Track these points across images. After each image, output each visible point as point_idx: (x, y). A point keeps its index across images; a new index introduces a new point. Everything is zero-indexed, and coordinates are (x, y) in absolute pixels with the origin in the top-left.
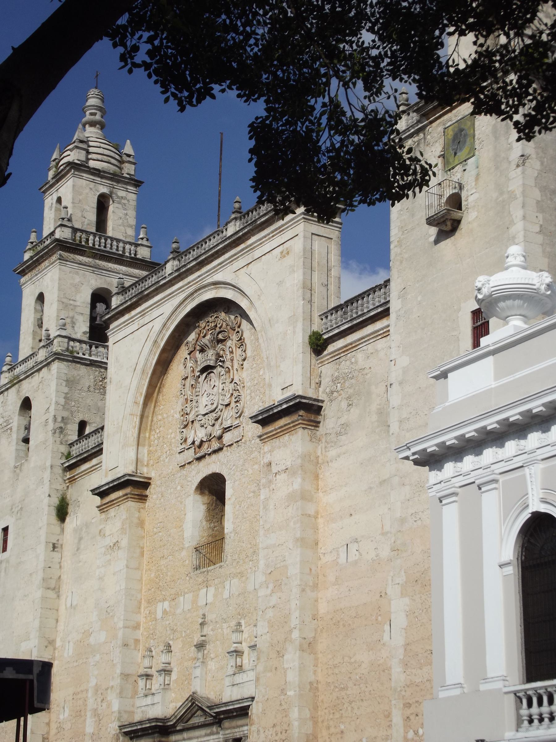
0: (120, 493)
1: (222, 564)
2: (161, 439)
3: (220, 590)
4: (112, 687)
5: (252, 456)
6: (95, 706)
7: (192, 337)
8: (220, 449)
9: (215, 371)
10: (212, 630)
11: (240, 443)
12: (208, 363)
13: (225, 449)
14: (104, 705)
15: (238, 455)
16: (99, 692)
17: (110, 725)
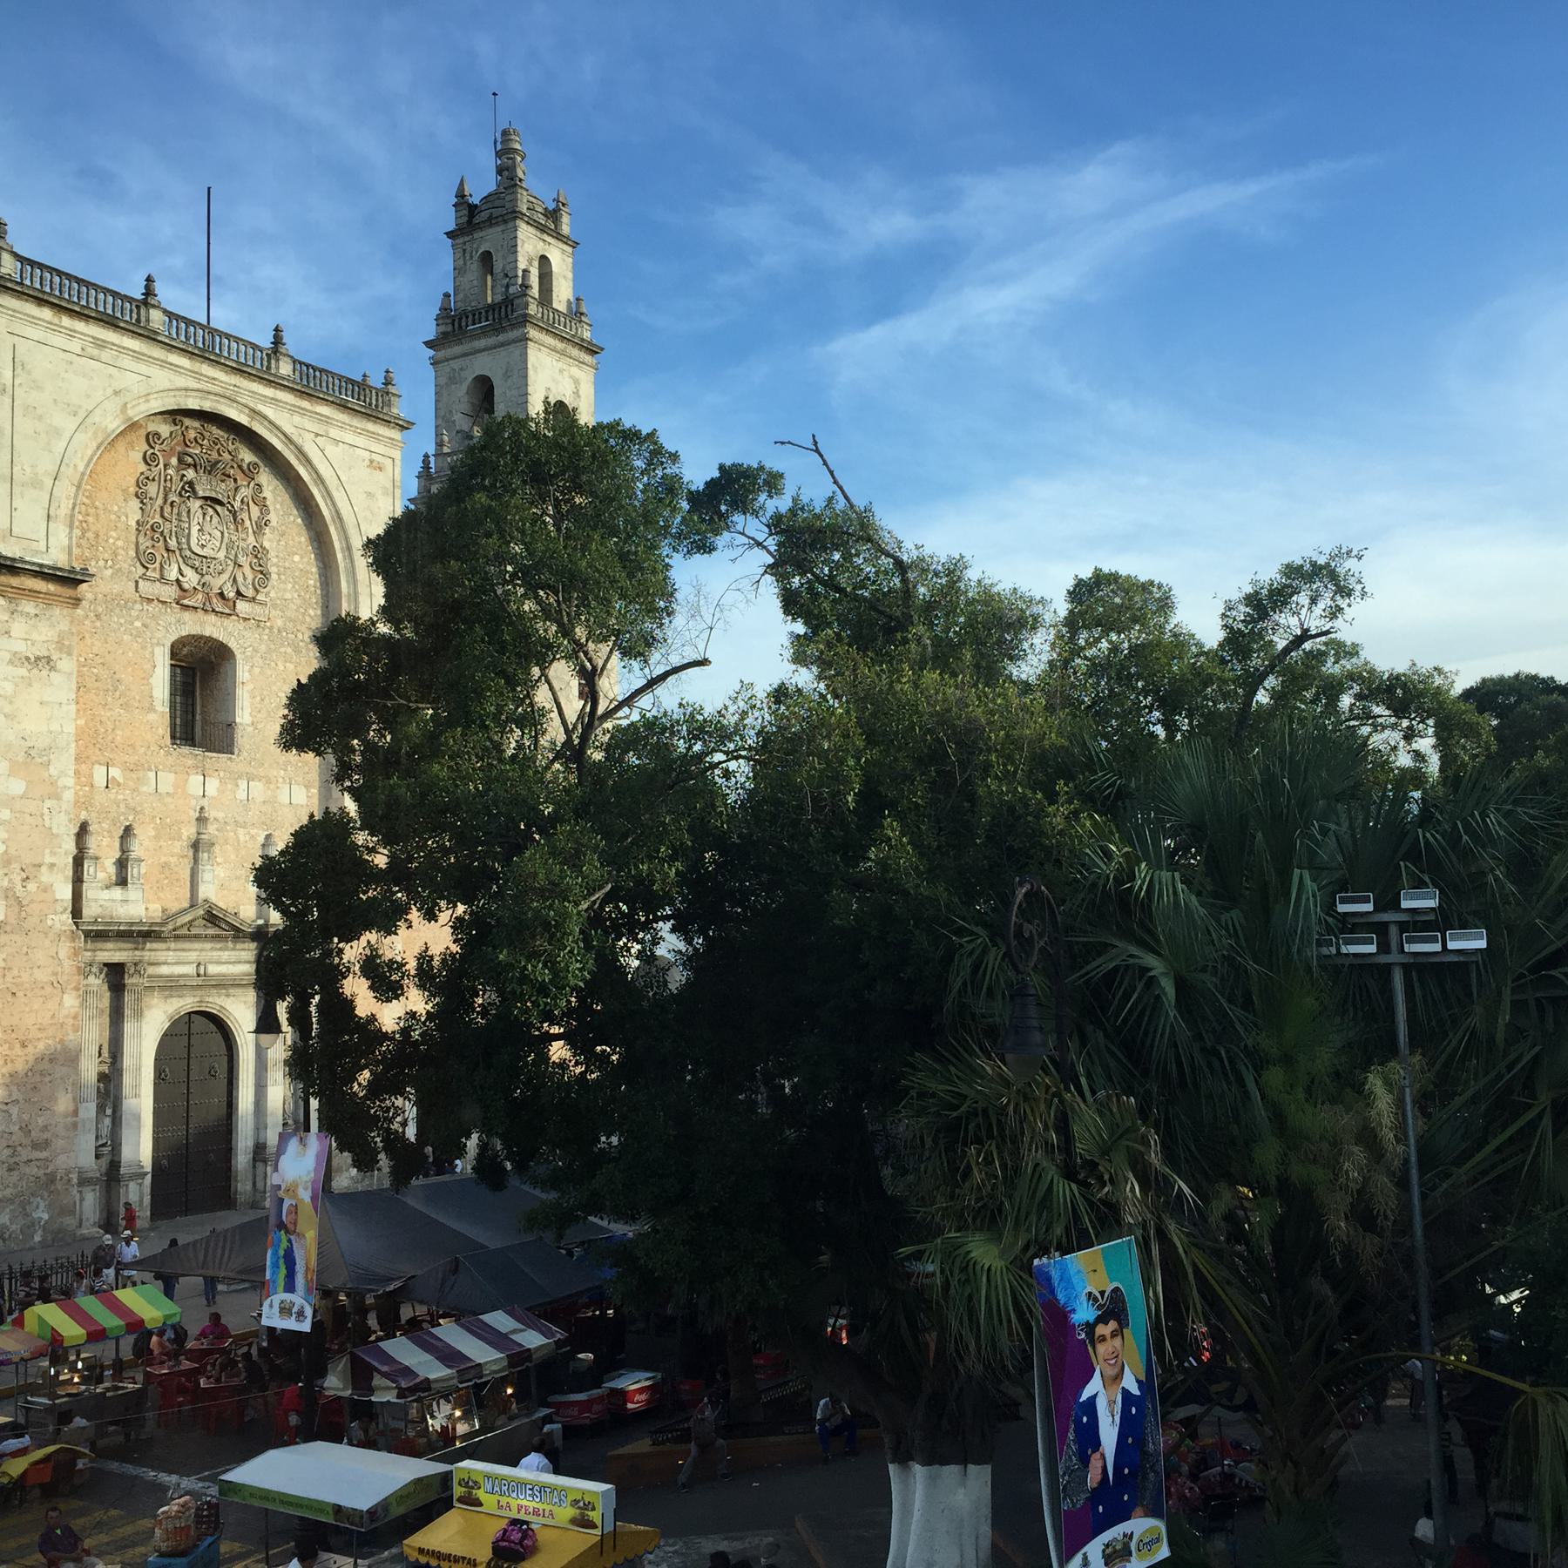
0: (52, 587)
1: (233, 757)
2: (90, 535)
3: (229, 786)
4: (52, 865)
5: (282, 650)
6: (5, 883)
7: (165, 429)
8: (230, 615)
9: (218, 508)
10: (217, 830)
11: (262, 624)
12: (220, 497)
13: (234, 617)
14: (32, 886)
15: (257, 636)
16: (16, 866)
17: (53, 916)
